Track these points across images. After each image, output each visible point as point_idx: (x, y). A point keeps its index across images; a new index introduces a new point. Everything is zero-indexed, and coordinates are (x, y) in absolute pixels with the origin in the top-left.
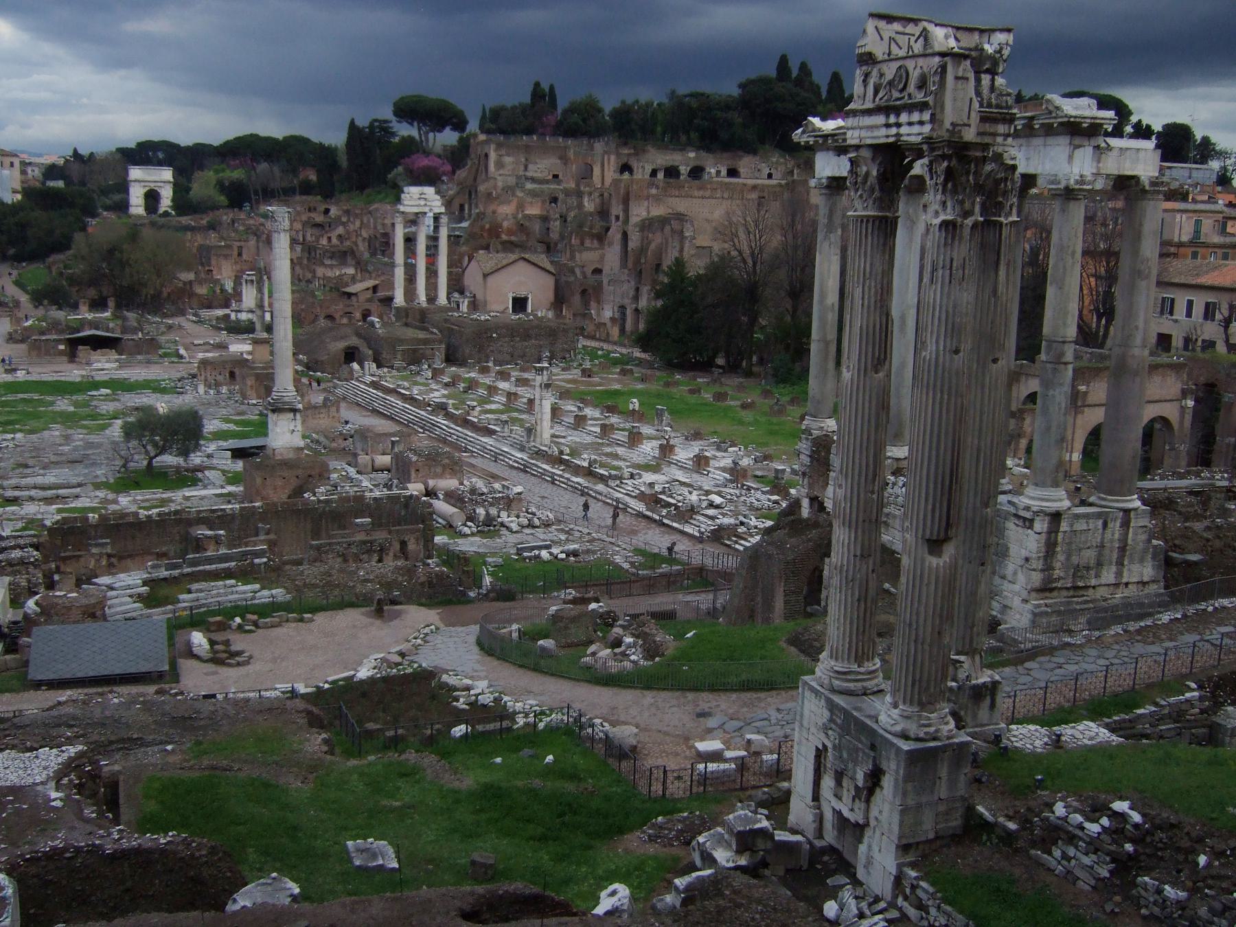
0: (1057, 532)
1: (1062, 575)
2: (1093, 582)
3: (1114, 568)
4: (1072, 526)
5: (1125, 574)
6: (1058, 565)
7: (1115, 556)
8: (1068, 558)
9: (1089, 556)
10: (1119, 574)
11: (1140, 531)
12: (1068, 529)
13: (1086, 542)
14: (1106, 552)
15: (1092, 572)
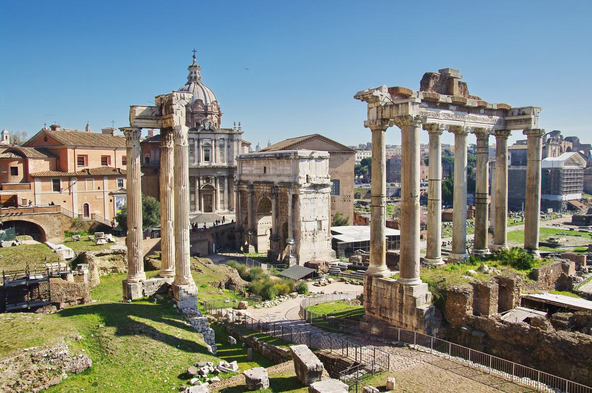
0: (371, 285)
1: (375, 306)
2: (389, 316)
3: (398, 314)
4: (377, 284)
5: (403, 318)
6: (373, 302)
8: (377, 299)
10: (400, 317)
12: (375, 285)
14: (393, 303)
15: (388, 311)
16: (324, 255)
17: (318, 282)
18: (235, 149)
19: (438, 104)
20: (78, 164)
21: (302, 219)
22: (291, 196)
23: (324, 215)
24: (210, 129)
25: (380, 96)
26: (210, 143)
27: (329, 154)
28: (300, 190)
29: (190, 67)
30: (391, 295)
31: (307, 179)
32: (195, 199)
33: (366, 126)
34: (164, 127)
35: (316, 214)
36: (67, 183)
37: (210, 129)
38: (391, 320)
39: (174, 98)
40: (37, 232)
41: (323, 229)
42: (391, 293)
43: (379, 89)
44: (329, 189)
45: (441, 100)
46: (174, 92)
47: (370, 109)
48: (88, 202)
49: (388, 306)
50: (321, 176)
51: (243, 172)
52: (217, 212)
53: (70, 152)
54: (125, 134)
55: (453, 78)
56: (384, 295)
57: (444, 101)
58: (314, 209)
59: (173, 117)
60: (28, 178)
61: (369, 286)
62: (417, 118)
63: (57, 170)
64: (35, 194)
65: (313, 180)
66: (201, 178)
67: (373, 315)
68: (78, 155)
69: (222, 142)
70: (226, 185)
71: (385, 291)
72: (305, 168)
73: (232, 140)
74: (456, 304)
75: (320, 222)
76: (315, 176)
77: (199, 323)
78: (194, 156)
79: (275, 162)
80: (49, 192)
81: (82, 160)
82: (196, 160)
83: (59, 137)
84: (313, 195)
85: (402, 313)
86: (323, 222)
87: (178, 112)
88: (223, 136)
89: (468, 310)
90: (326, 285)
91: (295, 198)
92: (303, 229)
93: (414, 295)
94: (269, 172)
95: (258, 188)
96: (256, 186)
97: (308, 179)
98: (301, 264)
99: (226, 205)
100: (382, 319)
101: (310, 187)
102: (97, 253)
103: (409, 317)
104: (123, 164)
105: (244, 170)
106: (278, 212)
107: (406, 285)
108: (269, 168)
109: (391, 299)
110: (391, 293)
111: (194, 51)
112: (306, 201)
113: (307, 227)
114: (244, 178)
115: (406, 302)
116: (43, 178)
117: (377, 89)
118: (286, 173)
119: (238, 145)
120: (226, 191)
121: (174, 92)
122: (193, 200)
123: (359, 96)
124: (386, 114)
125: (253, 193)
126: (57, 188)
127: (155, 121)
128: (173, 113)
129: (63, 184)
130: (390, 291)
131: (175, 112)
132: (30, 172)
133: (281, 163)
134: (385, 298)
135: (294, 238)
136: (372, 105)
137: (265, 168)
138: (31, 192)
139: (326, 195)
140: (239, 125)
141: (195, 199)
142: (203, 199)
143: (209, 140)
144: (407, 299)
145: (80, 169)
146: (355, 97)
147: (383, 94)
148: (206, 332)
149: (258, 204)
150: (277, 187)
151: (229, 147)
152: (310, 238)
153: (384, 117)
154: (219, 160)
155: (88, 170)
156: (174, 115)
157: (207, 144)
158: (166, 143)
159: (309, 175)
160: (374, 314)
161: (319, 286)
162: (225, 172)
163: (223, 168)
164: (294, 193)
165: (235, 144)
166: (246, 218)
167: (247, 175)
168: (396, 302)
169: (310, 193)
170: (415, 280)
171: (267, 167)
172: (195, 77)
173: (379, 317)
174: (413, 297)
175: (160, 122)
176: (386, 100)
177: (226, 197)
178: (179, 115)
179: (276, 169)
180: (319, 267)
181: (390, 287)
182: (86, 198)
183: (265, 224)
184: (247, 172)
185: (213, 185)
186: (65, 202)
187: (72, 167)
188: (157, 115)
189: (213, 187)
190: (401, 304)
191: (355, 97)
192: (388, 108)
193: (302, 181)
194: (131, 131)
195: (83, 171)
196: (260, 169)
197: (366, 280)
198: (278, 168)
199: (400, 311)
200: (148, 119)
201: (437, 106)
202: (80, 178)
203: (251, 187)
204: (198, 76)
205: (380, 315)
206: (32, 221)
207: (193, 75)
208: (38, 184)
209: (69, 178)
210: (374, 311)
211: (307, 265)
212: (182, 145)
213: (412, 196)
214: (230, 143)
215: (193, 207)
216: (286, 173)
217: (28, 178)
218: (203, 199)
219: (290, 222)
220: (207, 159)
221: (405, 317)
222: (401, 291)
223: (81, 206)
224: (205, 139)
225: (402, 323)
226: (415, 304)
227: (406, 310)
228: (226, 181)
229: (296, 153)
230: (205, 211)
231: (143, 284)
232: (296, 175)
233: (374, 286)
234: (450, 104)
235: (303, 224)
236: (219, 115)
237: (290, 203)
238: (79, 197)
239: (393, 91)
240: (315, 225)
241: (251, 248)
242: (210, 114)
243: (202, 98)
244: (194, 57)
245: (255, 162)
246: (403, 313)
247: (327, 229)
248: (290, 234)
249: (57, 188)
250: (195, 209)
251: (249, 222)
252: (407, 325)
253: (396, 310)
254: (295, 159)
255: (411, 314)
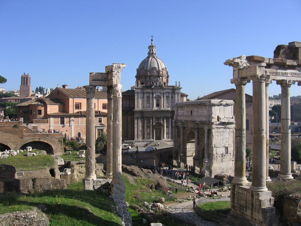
0: (235, 190)
1: (237, 205)
2: (245, 213)
3: (250, 211)
6: (236, 202)
7: (250, 207)
8: (238, 201)
9: (243, 203)
10: (252, 214)
11: (257, 201)
12: (237, 191)
13: (242, 197)
16: (229, 171)
17: (221, 189)
18: (176, 99)
19: (286, 67)
20: (75, 108)
21: (214, 146)
22: (207, 130)
23: (229, 143)
24: (160, 86)
25: (239, 62)
26: (160, 95)
27: (234, 102)
28: (213, 126)
29: (149, 47)
30: (246, 198)
31: (218, 119)
32: (150, 131)
33: (232, 83)
34: (109, 85)
35: (224, 143)
36: (68, 119)
37: (160, 86)
38: (247, 215)
39: (114, 68)
40: (49, 149)
41: (229, 153)
42: (246, 197)
43: (240, 58)
44: (233, 126)
45: (288, 64)
46: (113, 64)
47: (234, 71)
48: (81, 132)
49: (244, 205)
50: (228, 117)
51: (179, 114)
52: (164, 140)
53: (71, 100)
54: (86, 90)
55: (298, 48)
56: (242, 197)
57: (290, 64)
58: (223, 139)
59: (113, 79)
60: (47, 116)
61: (234, 191)
62: (262, 76)
63: (63, 112)
64: (50, 126)
65: (222, 119)
66: (154, 117)
67: (236, 211)
68: (75, 103)
69: (167, 95)
70: (170, 123)
71: (243, 195)
72: (216, 112)
73: (174, 93)
74: (291, 207)
75: (227, 148)
76: (223, 117)
77: (122, 208)
78: (149, 103)
79: (198, 107)
80: (58, 125)
81: (78, 106)
82: (151, 106)
83: (67, 93)
84: (222, 130)
85: (253, 211)
86: (229, 149)
87: (116, 76)
88: (167, 91)
89: (299, 212)
90: (226, 191)
91: (210, 131)
92: (214, 152)
93: (260, 198)
94: (194, 114)
95: (187, 125)
96: (186, 123)
97: (218, 118)
98: (213, 177)
99: (170, 136)
100: (241, 214)
101: (219, 124)
102: (78, 162)
103: (257, 214)
104: (103, 108)
105: (179, 113)
106: (199, 141)
107: (255, 191)
108: (194, 112)
109: (246, 201)
110: (246, 197)
111: (152, 37)
112: (217, 134)
113: (218, 151)
114: (179, 118)
115: (255, 203)
116: (55, 116)
117: (238, 58)
118: (204, 114)
119: (178, 97)
120: (170, 127)
121: (113, 64)
122: (148, 131)
123: (227, 63)
124: (244, 75)
125: (184, 128)
126: (62, 122)
127: (104, 82)
128: (113, 77)
129: (66, 120)
130: (245, 195)
131: (114, 76)
132: (48, 113)
133: (201, 108)
134: (243, 200)
135: (208, 159)
136: (236, 69)
137: (191, 111)
138: (48, 125)
139: (232, 130)
140: (179, 83)
141: (150, 131)
142: (155, 130)
143: (159, 93)
144: (256, 201)
145: (76, 111)
146: (226, 64)
147: (242, 61)
148: (126, 214)
149: (187, 135)
150: (198, 124)
151: (172, 97)
152: (219, 159)
153: (243, 76)
154: (165, 106)
155: (81, 112)
156: (113, 78)
157: (159, 96)
158: (110, 95)
159: (219, 116)
160: (236, 210)
161: (221, 192)
162: (169, 114)
163: (168, 111)
164: (209, 128)
165: (176, 96)
166: (180, 145)
167: (180, 116)
168: (249, 204)
169: (220, 128)
170: (262, 188)
171: (193, 111)
172: (153, 53)
173: (239, 213)
174: (259, 200)
175: (107, 82)
176: (245, 65)
177: (170, 131)
178: (116, 78)
179: (198, 112)
180: (224, 179)
181: (245, 192)
182: (79, 129)
183: (191, 148)
184: (181, 114)
185: (162, 122)
186: (67, 131)
187: (72, 110)
188: (105, 78)
189: (161, 123)
190: (252, 204)
191: (226, 64)
192: (245, 70)
193: (214, 120)
194: (89, 88)
195: (78, 112)
196: (189, 112)
197: (232, 187)
198: (199, 112)
199: (252, 210)
200: (100, 81)
201: (286, 68)
202: (76, 116)
203: (183, 124)
204: (154, 52)
205: (240, 212)
206: (46, 141)
207: (151, 52)
208: (52, 120)
209: (70, 116)
210: (236, 208)
211: (216, 177)
212: (118, 96)
213: (259, 130)
214: (173, 95)
215: (148, 137)
216: (204, 115)
217: (47, 116)
218: (155, 130)
219: (206, 147)
220: (158, 105)
221: (255, 214)
222: (252, 196)
223: (76, 133)
224: (156, 93)
225: (253, 218)
226: (260, 205)
227: (255, 209)
228: (170, 120)
229: (210, 102)
230: (156, 139)
231: (94, 182)
232: (210, 116)
233: (237, 191)
234: (296, 66)
235: (214, 149)
236: (168, 77)
237: (206, 135)
238: (75, 128)
239: (250, 59)
240: (223, 150)
241: (182, 164)
242: (161, 76)
243: (156, 66)
244: (152, 40)
245: (185, 107)
246: (254, 211)
247: (232, 153)
248: (206, 155)
249: (62, 122)
250: (150, 138)
251: (181, 147)
252: (256, 220)
253: (249, 209)
254: (210, 105)
255: (258, 212)
